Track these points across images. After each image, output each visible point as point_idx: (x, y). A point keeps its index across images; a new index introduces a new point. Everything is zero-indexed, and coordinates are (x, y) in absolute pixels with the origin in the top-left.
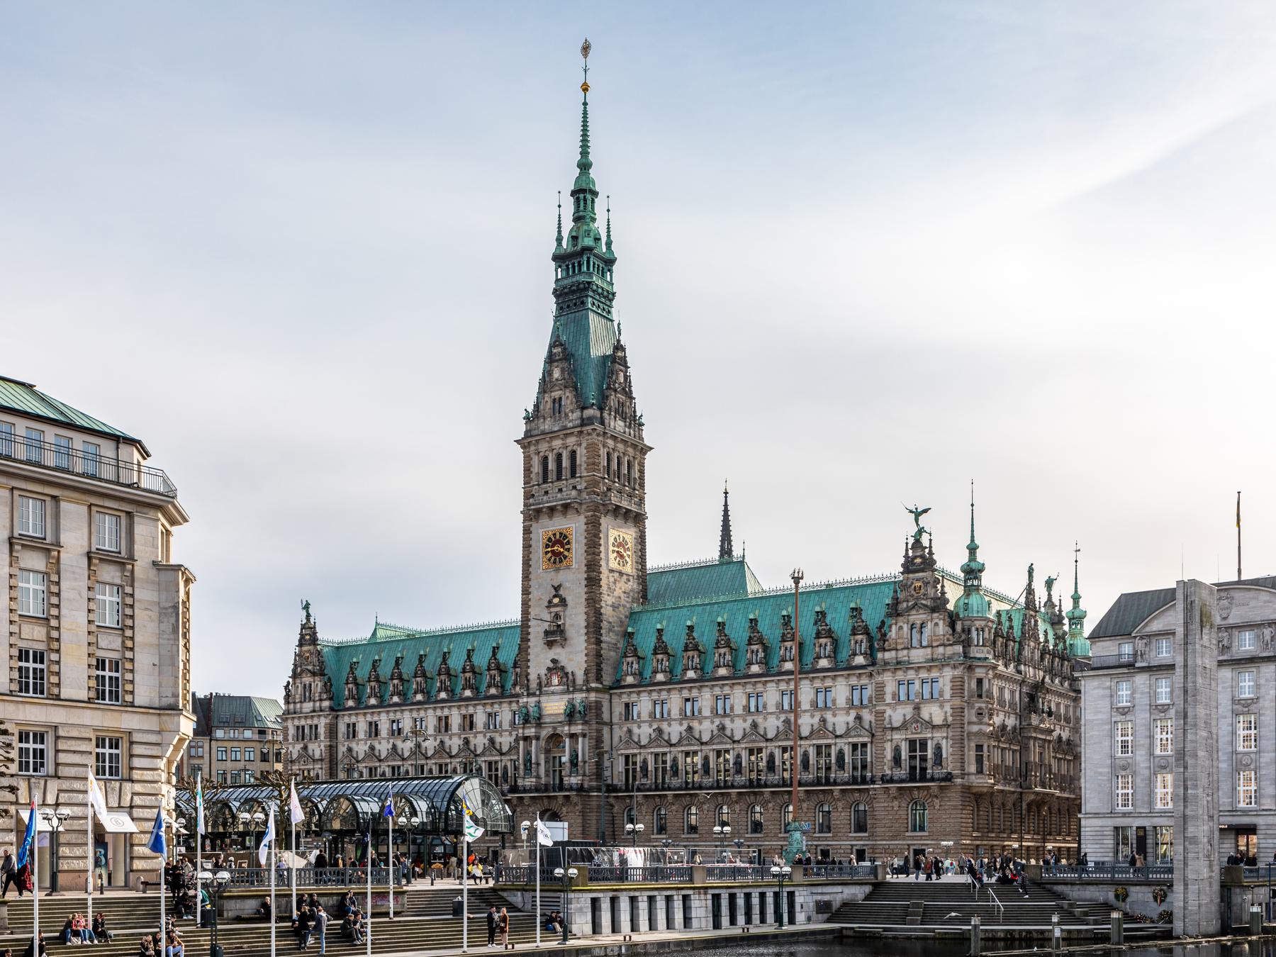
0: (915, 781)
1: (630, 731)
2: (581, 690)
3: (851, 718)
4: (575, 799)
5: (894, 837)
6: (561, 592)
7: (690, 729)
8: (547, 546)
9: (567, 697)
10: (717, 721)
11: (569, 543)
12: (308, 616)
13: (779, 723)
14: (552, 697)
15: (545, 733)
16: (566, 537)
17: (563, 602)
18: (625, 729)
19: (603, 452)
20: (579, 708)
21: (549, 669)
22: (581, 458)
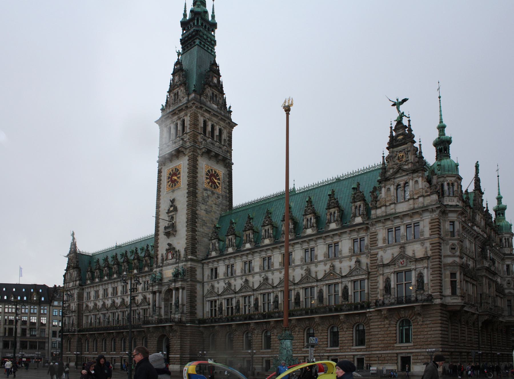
0: (401, 303)
1: (213, 287)
2: (183, 261)
3: (353, 263)
4: (175, 328)
5: (386, 348)
6: (174, 204)
7: (247, 281)
8: (169, 178)
9: (175, 266)
10: (263, 275)
11: (179, 173)
12: (74, 239)
13: (303, 272)
14: (169, 267)
15: (164, 289)
16: (178, 170)
17: (176, 209)
18: (210, 285)
19: (201, 120)
20: (181, 270)
21: (167, 250)
22: (187, 123)
